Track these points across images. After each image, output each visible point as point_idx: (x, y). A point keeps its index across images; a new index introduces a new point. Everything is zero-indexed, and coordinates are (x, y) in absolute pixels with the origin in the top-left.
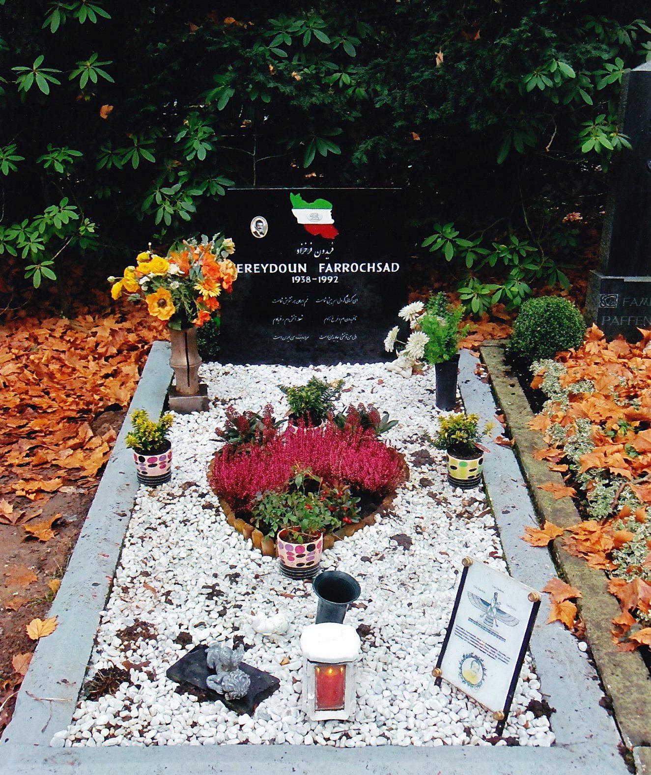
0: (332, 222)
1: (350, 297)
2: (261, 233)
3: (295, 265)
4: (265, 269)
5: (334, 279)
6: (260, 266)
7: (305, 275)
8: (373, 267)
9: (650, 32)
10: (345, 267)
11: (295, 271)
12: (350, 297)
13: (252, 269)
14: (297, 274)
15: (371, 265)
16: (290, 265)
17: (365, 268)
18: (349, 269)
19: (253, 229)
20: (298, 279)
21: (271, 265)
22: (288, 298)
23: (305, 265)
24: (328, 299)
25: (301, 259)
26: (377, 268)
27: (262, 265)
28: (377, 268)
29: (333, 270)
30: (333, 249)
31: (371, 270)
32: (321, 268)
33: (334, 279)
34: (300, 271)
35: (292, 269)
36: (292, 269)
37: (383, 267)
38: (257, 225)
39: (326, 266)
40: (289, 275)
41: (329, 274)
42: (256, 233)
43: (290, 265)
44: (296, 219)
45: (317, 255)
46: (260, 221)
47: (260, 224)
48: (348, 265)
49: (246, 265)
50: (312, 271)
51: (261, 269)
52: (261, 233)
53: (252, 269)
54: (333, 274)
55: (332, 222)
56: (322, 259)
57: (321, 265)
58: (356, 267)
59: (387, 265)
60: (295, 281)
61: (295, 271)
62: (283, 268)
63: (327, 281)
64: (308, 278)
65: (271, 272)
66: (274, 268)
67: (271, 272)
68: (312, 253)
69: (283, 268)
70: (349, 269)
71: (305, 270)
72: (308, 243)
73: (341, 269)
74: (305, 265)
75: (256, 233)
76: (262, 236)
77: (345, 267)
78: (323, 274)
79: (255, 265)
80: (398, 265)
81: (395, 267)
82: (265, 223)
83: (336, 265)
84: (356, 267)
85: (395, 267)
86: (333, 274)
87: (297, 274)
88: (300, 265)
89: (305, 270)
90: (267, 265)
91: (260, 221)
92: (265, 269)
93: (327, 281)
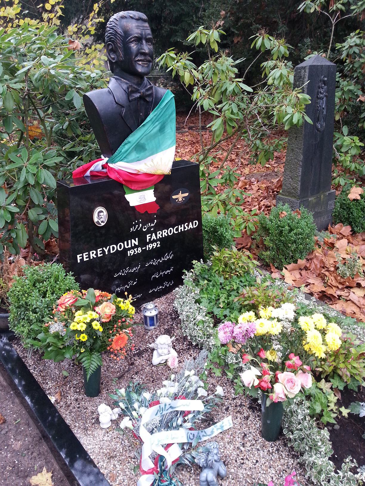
2: (102, 222)
3: (129, 241)
4: (106, 251)
5: (157, 244)
6: (103, 251)
8: (182, 228)
10: (165, 233)
11: (130, 246)
12: (168, 255)
13: (96, 254)
14: (132, 248)
15: (181, 227)
16: (126, 242)
17: (177, 230)
18: (167, 233)
19: (96, 219)
20: (131, 253)
21: (111, 247)
22: (126, 269)
23: (137, 239)
24: (154, 261)
25: (133, 236)
26: (185, 228)
27: (104, 248)
28: (185, 228)
29: (156, 237)
30: (155, 221)
32: (148, 238)
33: (157, 244)
34: (133, 245)
35: (128, 245)
36: (128, 245)
37: (188, 226)
40: (125, 250)
41: (154, 241)
42: (98, 222)
43: (126, 242)
45: (145, 228)
46: (102, 212)
47: (102, 214)
49: (91, 252)
50: (143, 243)
51: (103, 252)
52: (102, 222)
53: (96, 254)
55: (154, 199)
56: (149, 231)
57: (148, 236)
60: (130, 254)
61: (130, 246)
65: (112, 252)
66: (113, 248)
67: (112, 252)
70: (167, 233)
71: (137, 243)
72: (138, 221)
73: (162, 235)
74: (137, 239)
75: (98, 222)
76: (103, 224)
77: (165, 233)
78: (151, 242)
80: (197, 221)
82: (105, 213)
83: (158, 233)
86: (154, 241)
87: (132, 248)
88: (133, 240)
89: (137, 243)
90: (108, 247)
91: (102, 212)
92: (106, 251)
93: (153, 247)
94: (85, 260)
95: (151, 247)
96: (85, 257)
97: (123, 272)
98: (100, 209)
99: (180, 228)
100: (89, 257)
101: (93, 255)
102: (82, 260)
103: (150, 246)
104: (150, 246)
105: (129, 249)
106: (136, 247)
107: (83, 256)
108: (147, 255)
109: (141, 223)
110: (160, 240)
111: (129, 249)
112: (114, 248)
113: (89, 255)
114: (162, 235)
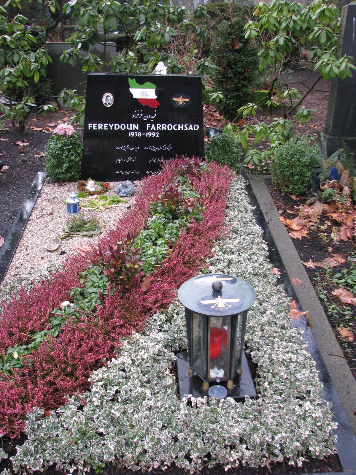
0: (155, 97)
1: (167, 146)
2: (109, 104)
3: (131, 125)
4: (111, 127)
5: (156, 134)
6: (108, 126)
7: (138, 131)
8: (182, 127)
9: (132, 90)
10: (164, 127)
11: (131, 129)
13: (103, 127)
14: (132, 131)
15: (181, 126)
16: (128, 125)
17: (177, 127)
18: (167, 128)
19: (104, 101)
20: (131, 134)
21: (115, 125)
24: (152, 148)
25: (135, 121)
26: (184, 128)
28: (184, 128)
31: (181, 129)
33: (156, 134)
35: (129, 127)
36: (129, 127)
37: (188, 127)
38: (106, 99)
39: (151, 126)
40: (127, 131)
41: (153, 131)
42: (106, 103)
43: (128, 125)
44: (132, 95)
45: (145, 118)
47: (109, 98)
48: (166, 126)
49: (99, 125)
50: (143, 129)
51: (109, 127)
52: (109, 104)
53: (103, 127)
54: (156, 131)
55: (155, 97)
56: (149, 121)
57: (148, 125)
58: (171, 127)
59: (191, 126)
61: (131, 129)
62: (123, 127)
63: (152, 135)
64: (140, 134)
65: (115, 129)
66: (117, 127)
67: (115, 129)
68: (142, 117)
69: (123, 127)
70: (167, 128)
71: (137, 128)
72: (140, 111)
73: (161, 128)
75: (106, 103)
76: (109, 106)
77: (164, 127)
78: (150, 131)
79: (105, 125)
80: (198, 126)
81: (196, 127)
82: (111, 97)
83: (157, 125)
84: (171, 127)
85: (196, 127)
86: (156, 131)
87: (132, 131)
88: (134, 126)
89: (137, 128)
92: (111, 127)
93: (152, 135)
94: (94, 129)
95: (150, 135)
96: (94, 127)
97: (124, 147)
98: (108, 94)
99: (179, 127)
100: (97, 127)
101: (100, 127)
102: (92, 128)
103: (150, 134)
104: (150, 134)
105: (131, 131)
106: (136, 130)
107: (92, 125)
108: (144, 141)
109: (142, 113)
110: (160, 131)
111: (131, 131)
112: (117, 127)
113: (97, 126)
114: (161, 128)
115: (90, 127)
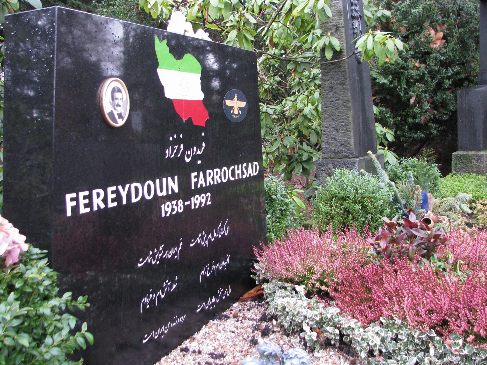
3: (164, 180)
6: (117, 192)
11: (164, 193)
16: (158, 181)
19: (107, 108)
20: (166, 209)
21: (133, 185)
22: (158, 250)
23: (176, 177)
27: (120, 187)
30: (204, 144)
34: (170, 193)
38: (113, 98)
40: (158, 201)
42: (111, 114)
43: (158, 181)
44: (162, 88)
46: (119, 91)
47: (118, 95)
49: (95, 192)
51: (118, 198)
52: (120, 116)
60: (166, 212)
65: (134, 200)
67: (134, 200)
74: (176, 177)
75: (111, 114)
79: (110, 189)
90: (127, 186)
91: (119, 91)
92: (124, 194)
94: (83, 210)
95: (198, 202)
96: (82, 202)
97: (154, 255)
100: (90, 205)
102: (75, 209)
107: (76, 199)
108: (192, 220)
113: (90, 197)
115: (70, 204)
